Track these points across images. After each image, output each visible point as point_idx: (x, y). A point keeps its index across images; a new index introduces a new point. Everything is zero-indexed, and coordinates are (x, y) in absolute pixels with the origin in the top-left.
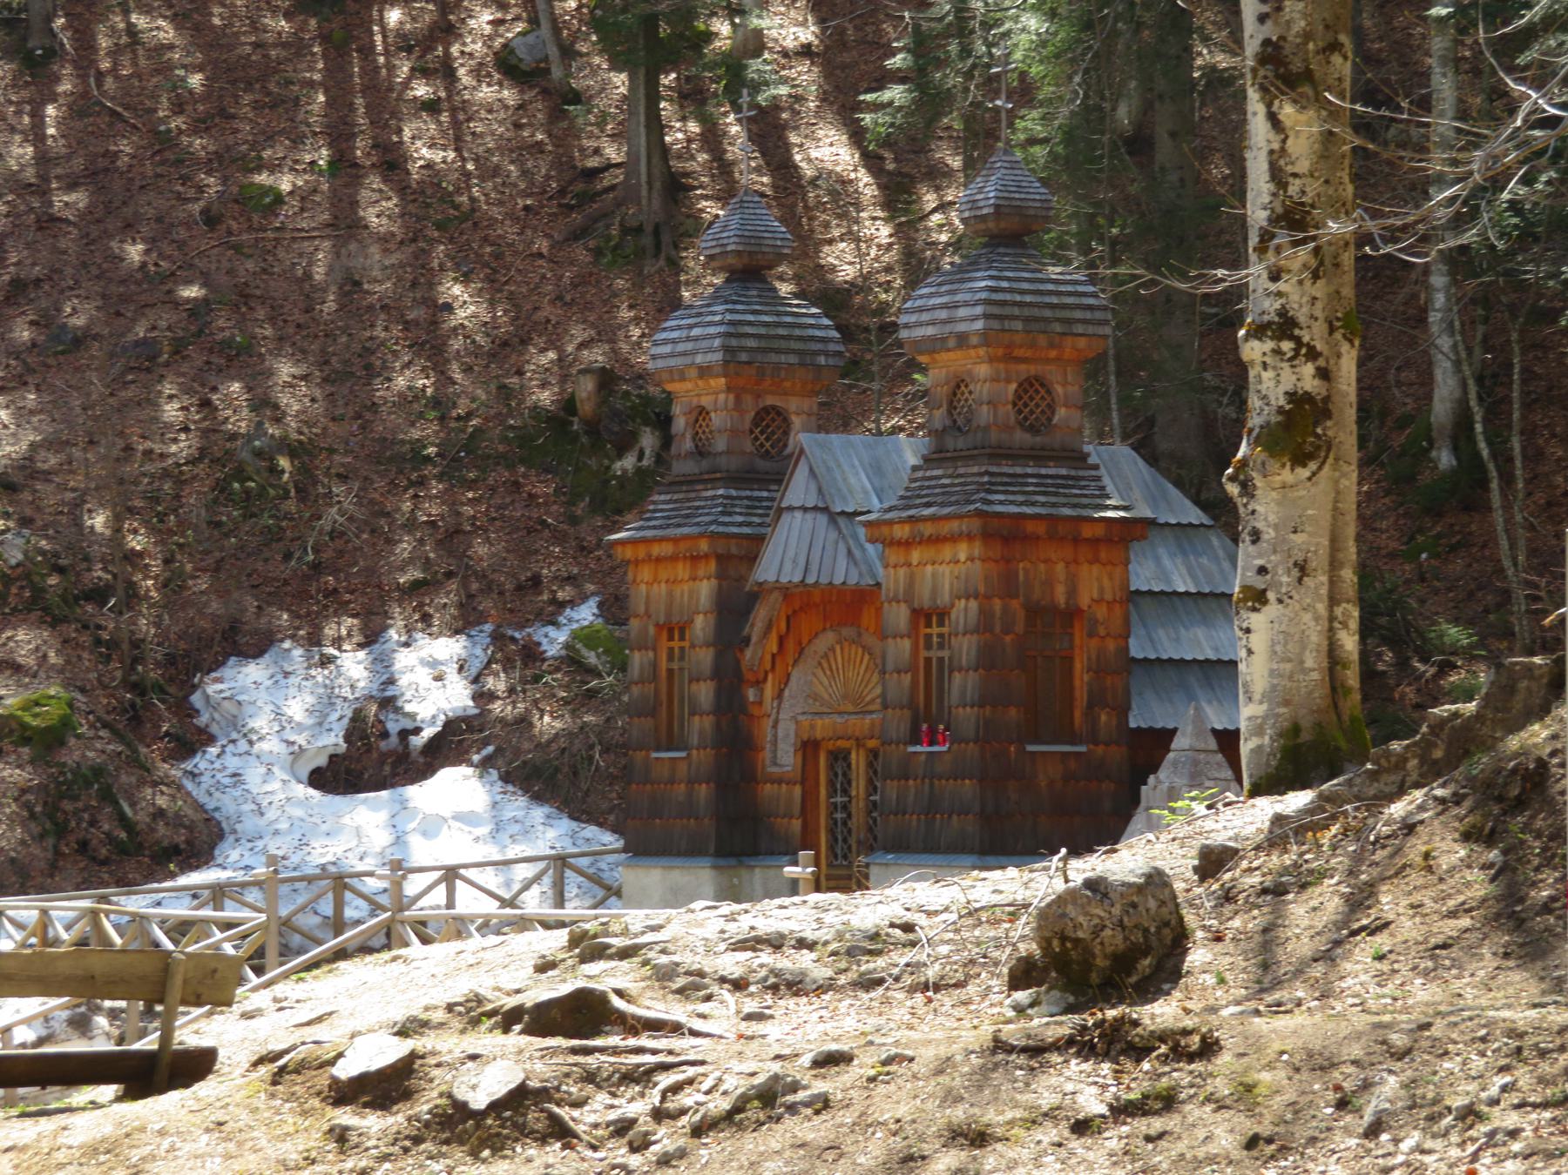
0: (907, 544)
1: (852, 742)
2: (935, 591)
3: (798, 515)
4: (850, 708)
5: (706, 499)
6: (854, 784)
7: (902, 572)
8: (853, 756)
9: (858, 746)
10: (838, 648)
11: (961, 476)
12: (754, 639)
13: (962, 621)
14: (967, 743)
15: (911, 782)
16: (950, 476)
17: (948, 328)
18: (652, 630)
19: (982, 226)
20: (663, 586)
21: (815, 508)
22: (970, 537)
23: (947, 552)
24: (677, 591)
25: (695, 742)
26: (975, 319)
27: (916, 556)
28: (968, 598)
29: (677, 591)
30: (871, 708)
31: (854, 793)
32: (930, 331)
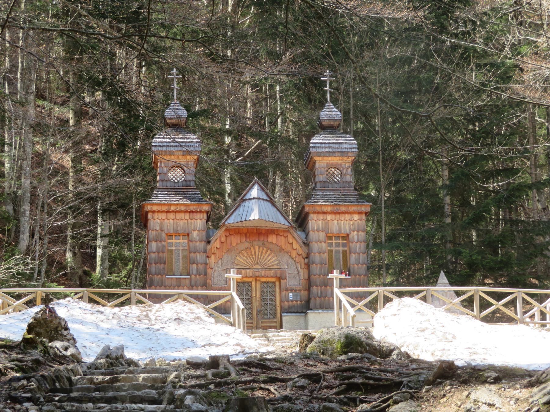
0: (324, 213)
1: (254, 279)
2: (339, 228)
3: (262, 201)
4: (260, 267)
5: (189, 194)
6: (254, 293)
7: (320, 222)
8: (253, 283)
9: (256, 280)
10: (252, 248)
11: (344, 195)
12: (212, 242)
13: (356, 237)
14: (360, 275)
15: (328, 287)
16: (338, 195)
17: (339, 150)
18: (164, 235)
19: (332, 123)
20: (171, 221)
21: (266, 200)
22: (360, 213)
23: (347, 216)
24: (181, 223)
25: (195, 272)
26: (353, 148)
27: (329, 217)
28: (358, 231)
29: (181, 223)
30: (271, 267)
31: (254, 295)
32: (327, 150)
